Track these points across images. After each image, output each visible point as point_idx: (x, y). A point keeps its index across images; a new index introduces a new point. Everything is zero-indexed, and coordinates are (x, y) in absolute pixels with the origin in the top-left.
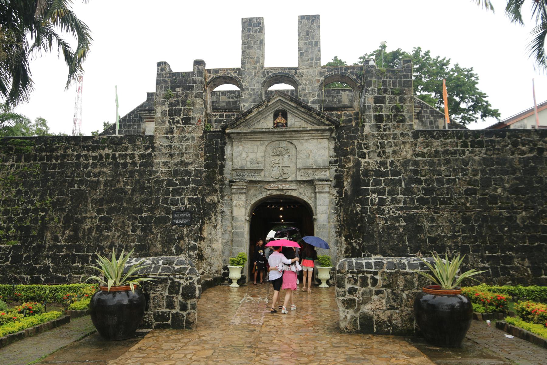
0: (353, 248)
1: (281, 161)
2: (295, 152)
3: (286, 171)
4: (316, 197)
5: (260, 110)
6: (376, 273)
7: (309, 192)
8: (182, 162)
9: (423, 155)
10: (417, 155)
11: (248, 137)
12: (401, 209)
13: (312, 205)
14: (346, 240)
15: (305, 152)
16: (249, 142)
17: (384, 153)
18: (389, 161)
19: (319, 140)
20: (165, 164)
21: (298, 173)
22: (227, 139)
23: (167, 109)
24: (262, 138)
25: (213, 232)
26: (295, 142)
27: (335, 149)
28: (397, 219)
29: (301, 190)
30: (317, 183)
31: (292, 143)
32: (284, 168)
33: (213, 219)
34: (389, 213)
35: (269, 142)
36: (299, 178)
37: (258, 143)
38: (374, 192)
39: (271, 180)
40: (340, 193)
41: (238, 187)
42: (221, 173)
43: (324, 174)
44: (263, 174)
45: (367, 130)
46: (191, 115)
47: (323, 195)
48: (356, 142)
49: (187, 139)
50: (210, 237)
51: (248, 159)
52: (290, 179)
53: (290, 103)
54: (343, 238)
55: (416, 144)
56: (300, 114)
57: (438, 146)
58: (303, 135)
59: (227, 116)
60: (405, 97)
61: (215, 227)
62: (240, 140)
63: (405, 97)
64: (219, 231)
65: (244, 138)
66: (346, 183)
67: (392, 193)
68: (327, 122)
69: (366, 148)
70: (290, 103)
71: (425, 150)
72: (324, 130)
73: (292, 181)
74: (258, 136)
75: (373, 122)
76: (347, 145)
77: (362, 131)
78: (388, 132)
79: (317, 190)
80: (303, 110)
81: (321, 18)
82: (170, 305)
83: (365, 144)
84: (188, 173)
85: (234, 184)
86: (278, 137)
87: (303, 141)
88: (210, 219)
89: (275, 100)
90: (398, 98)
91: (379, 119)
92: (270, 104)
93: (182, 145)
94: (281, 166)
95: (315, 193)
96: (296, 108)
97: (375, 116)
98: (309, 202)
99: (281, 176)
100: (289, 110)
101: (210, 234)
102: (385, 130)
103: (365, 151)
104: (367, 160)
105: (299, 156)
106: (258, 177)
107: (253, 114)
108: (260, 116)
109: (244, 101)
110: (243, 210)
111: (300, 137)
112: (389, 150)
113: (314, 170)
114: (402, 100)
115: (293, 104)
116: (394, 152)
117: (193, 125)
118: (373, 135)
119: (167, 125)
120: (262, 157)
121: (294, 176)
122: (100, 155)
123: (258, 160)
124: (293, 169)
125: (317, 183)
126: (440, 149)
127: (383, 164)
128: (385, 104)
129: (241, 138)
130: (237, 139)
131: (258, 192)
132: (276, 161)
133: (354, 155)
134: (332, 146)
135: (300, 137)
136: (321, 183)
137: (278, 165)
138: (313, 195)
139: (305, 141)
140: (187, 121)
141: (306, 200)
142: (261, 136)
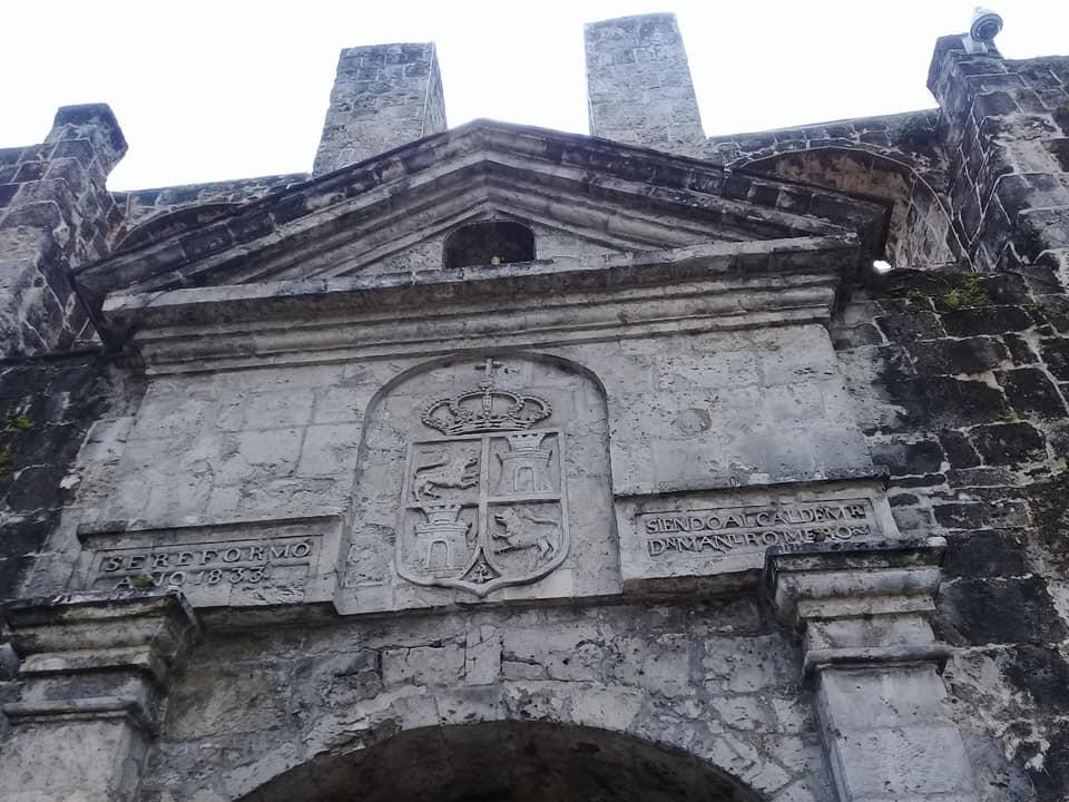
1: (487, 468)
2: (597, 415)
3: (519, 531)
4: (818, 732)
5: (362, 203)
7: (740, 685)
11: (262, 342)
15: (665, 401)
16: (263, 379)
19: (762, 337)
21: (625, 528)
22: (119, 389)
24: (351, 346)
26: (585, 355)
27: (891, 383)
29: (668, 674)
30: (807, 582)
31: (566, 367)
32: (507, 514)
35: (405, 365)
36: (638, 567)
37: (328, 376)
39: (404, 600)
41: (85, 658)
43: (849, 521)
44: (326, 554)
47: (889, 687)
51: (234, 469)
52: (562, 586)
53: (547, 170)
56: (615, 222)
58: (647, 309)
62: (201, 365)
65: (230, 353)
68: (798, 221)
70: (547, 170)
72: (783, 264)
73: (575, 608)
74: (329, 336)
76: (970, 358)
79: (818, 647)
80: (629, 187)
81: (684, 27)
85: (44, 635)
86: (465, 334)
87: (647, 348)
89: (456, 165)
92: (419, 181)
94: (483, 499)
95: (806, 685)
96: (584, 188)
99: (483, 567)
100: (548, 213)
106: (280, 575)
107: (309, 223)
108: (360, 245)
111: (625, 322)
113: (762, 502)
115: (563, 173)
120: (339, 451)
121: (593, 561)
123: (307, 470)
124: (583, 505)
125: (807, 582)
129: (206, 356)
130: (178, 359)
131: (266, 714)
132: (454, 474)
134: (864, 366)
135: (625, 322)
136: (841, 580)
137: (469, 497)
138: (787, 714)
139: (660, 344)
141: (723, 754)
142: (348, 335)
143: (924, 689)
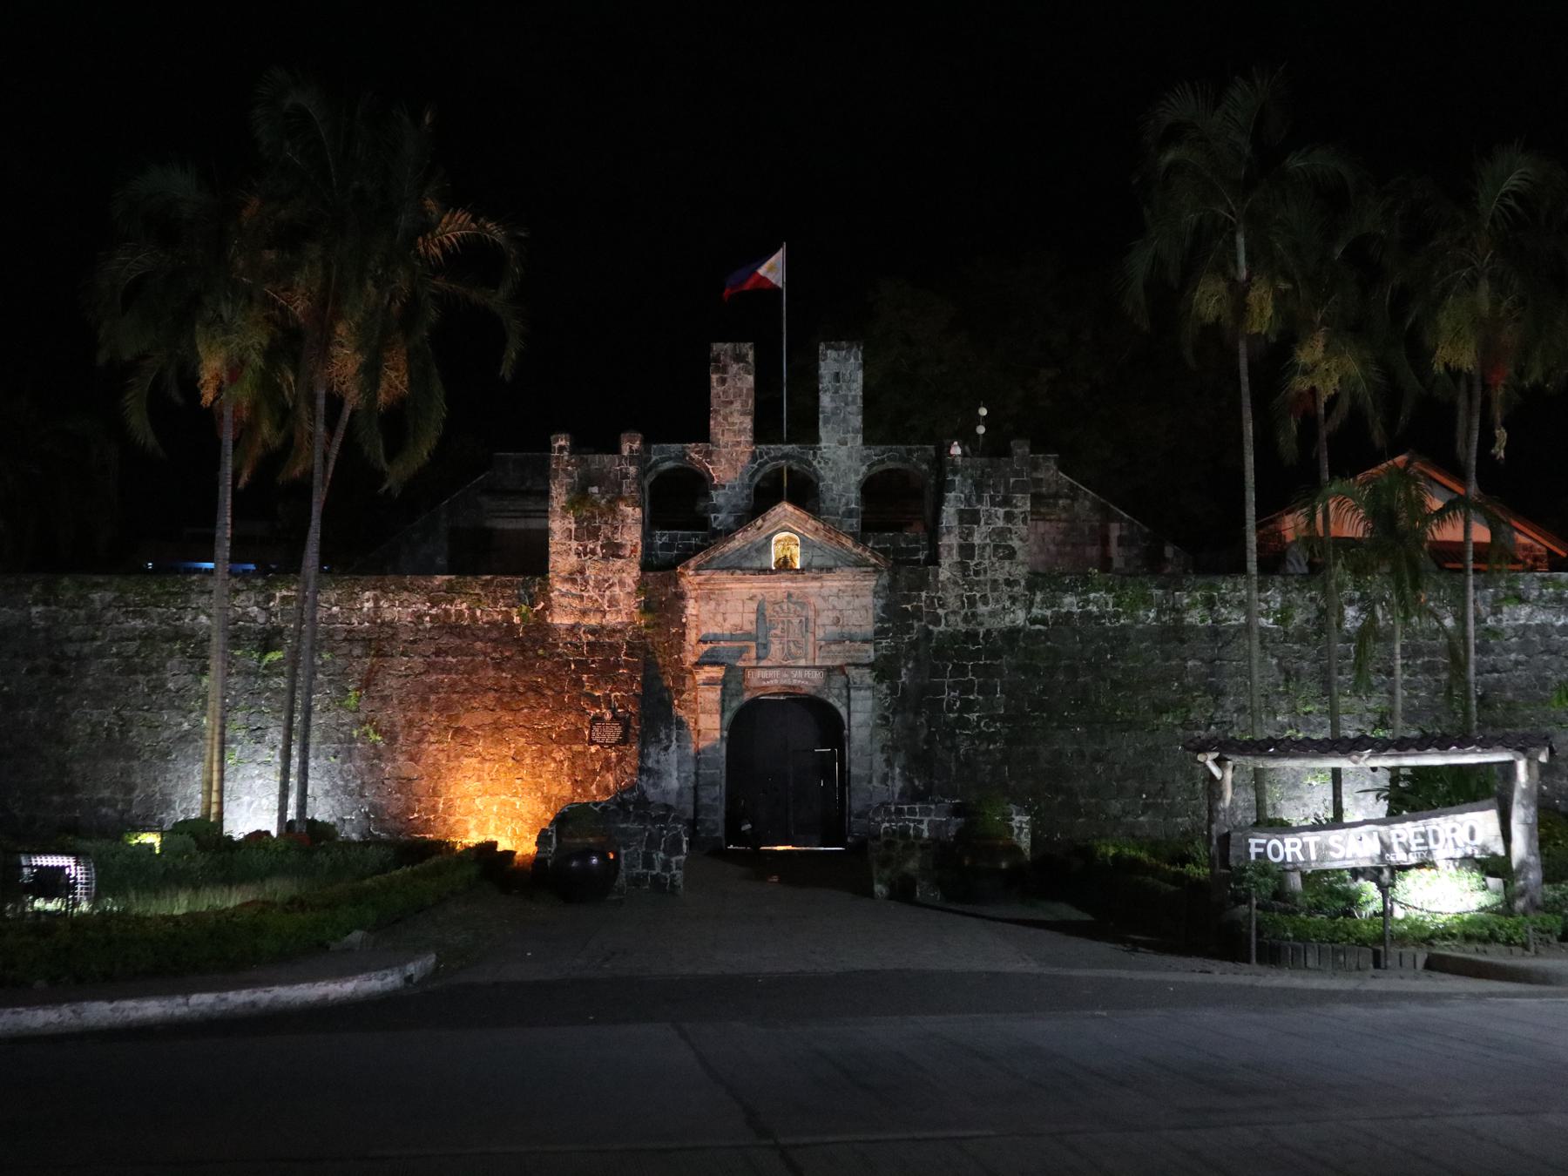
0: (915, 788)
6: (921, 822)
8: (603, 627)
9: (1043, 621)
10: (1034, 621)
12: (1002, 718)
13: (843, 711)
14: (902, 774)
17: (974, 615)
18: (982, 631)
20: (572, 629)
23: (573, 526)
25: (662, 758)
28: (991, 738)
33: (662, 736)
34: (978, 726)
38: (952, 688)
40: (893, 689)
42: (681, 649)
45: (944, 574)
46: (618, 539)
48: (924, 594)
49: (611, 586)
50: (656, 767)
54: (898, 770)
55: (1032, 604)
57: (1072, 604)
59: (683, 538)
60: (1016, 511)
61: (666, 749)
63: (1016, 511)
64: (673, 755)
66: (904, 671)
67: (986, 690)
69: (941, 606)
71: (1048, 613)
75: (956, 558)
77: (936, 575)
78: (982, 578)
82: (649, 863)
83: (940, 599)
84: (615, 648)
88: (657, 735)
90: (1001, 511)
91: (967, 550)
93: (602, 596)
97: (961, 547)
98: (837, 704)
101: (658, 762)
102: (977, 573)
103: (940, 611)
104: (942, 628)
105: (819, 622)
109: (717, 509)
110: (717, 718)
112: (982, 609)
114: (1009, 517)
116: (993, 614)
117: (620, 557)
118: (956, 583)
119: (573, 559)
121: (810, 656)
122: (446, 611)
126: (1075, 609)
127: (971, 636)
128: (978, 523)
133: (920, 620)
140: (613, 550)
143: (869, 693)
